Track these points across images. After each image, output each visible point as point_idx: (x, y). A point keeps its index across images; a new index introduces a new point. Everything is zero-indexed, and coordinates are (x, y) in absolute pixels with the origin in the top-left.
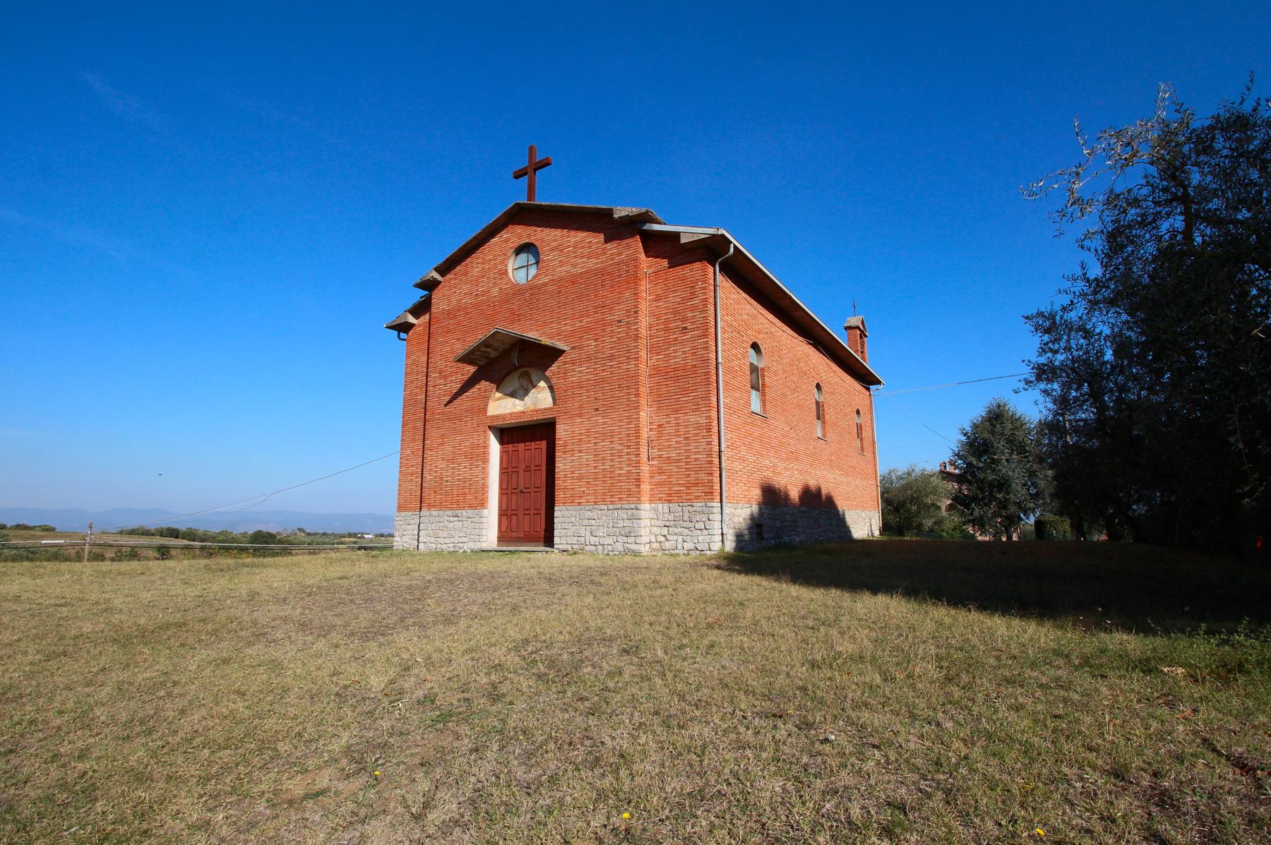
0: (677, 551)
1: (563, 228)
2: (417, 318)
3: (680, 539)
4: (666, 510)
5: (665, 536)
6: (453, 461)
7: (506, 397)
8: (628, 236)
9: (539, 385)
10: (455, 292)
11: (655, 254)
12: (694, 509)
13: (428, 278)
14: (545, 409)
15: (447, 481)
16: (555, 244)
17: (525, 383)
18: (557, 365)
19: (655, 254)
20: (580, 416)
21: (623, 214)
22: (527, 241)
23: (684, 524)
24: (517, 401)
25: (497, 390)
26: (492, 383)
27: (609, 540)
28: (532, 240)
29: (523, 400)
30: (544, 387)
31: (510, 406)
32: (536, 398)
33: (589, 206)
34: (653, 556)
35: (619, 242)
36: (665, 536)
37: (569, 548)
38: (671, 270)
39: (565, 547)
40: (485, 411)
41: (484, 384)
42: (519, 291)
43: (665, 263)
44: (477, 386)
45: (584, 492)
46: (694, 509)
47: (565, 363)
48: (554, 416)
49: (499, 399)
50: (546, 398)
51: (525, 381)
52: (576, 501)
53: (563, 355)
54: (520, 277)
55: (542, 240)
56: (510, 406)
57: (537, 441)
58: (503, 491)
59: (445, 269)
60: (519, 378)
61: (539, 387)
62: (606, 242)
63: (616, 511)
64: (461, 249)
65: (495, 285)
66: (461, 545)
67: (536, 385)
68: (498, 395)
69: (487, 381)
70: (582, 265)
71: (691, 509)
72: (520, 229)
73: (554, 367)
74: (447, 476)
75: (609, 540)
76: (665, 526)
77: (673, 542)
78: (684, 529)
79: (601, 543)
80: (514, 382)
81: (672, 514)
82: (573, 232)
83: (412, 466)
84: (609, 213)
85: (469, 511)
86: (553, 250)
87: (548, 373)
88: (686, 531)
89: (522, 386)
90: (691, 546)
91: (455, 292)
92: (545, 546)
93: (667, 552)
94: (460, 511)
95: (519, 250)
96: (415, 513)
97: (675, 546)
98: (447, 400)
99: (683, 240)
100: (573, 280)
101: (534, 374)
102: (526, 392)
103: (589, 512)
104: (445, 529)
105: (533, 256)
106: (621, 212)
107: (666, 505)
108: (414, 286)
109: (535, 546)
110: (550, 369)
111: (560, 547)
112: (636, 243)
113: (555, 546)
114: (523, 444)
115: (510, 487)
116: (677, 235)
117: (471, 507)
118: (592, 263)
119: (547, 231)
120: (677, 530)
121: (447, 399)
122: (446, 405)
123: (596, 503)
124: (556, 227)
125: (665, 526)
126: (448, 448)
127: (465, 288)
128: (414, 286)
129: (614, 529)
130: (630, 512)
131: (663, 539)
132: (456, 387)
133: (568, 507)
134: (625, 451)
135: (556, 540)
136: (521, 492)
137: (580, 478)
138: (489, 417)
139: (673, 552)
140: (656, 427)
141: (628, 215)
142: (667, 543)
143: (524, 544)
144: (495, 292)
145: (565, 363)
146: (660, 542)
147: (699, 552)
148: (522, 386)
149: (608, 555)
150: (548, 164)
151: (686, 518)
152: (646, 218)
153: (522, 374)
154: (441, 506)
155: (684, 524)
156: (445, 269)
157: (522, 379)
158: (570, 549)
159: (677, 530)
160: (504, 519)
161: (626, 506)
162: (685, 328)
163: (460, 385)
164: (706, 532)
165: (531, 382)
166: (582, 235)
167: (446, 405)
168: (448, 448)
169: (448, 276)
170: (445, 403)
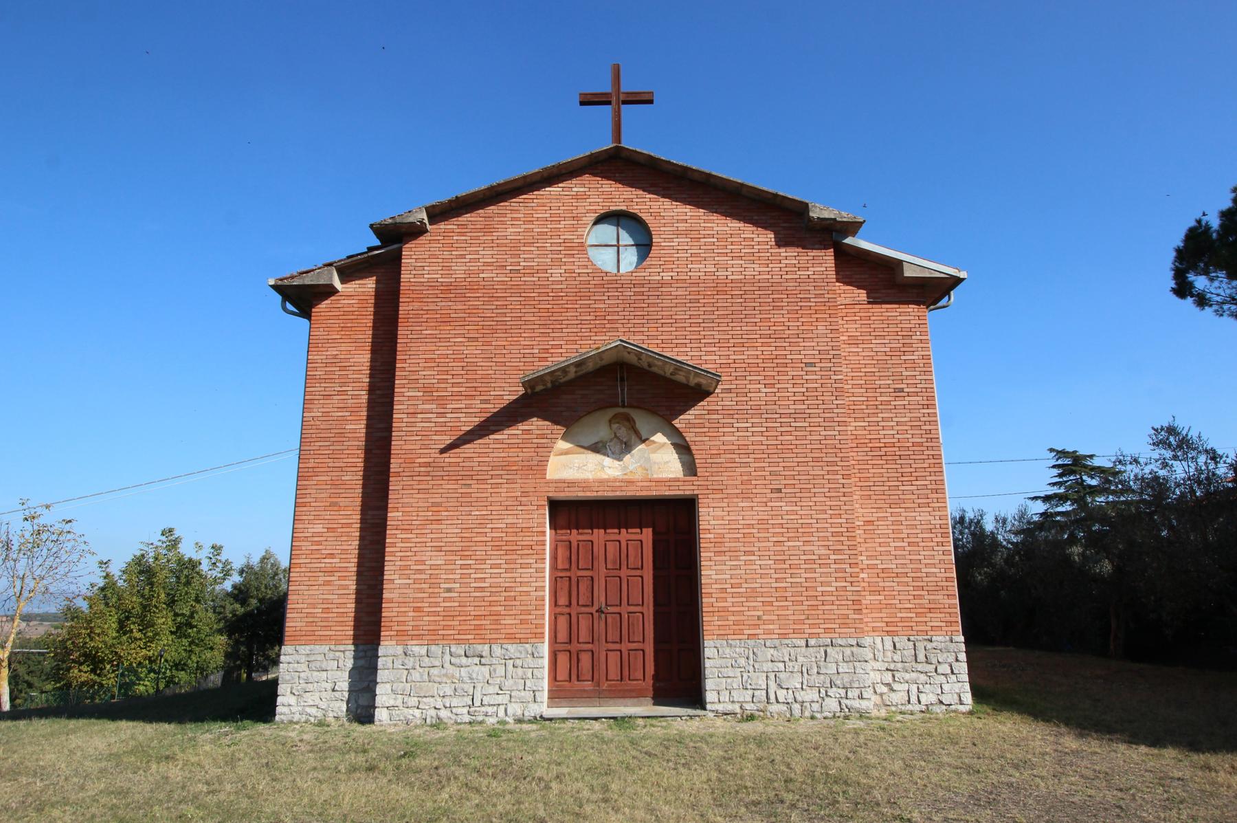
0: (910, 707)
1: (698, 205)
2: (343, 282)
3: (914, 688)
4: (889, 645)
5: (888, 685)
6: (462, 553)
7: (582, 450)
8: (817, 246)
9: (652, 439)
10: (463, 256)
11: (847, 280)
12: (934, 645)
13: (411, 219)
14: (670, 480)
15: (449, 590)
16: (682, 226)
17: (623, 432)
18: (697, 412)
19: (847, 280)
20: (745, 496)
21: (826, 215)
22: (624, 208)
23: (920, 667)
24: (607, 461)
25: (564, 438)
26: (556, 422)
27: (812, 695)
28: (634, 209)
29: (620, 459)
30: (664, 445)
31: (591, 466)
32: (648, 460)
33: (765, 188)
34: (825, 718)
35: (800, 250)
36: (888, 685)
37: (737, 708)
38: (870, 306)
39: (729, 707)
40: (543, 472)
41: (536, 425)
42: (609, 283)
43: (862, 295)
44: (522, 426)
45: (759, 618)
46: (934, 645)
47: (710, 412)
48: (696, 492)
49: (566, 453)
50: (667, 462)
51: (623, 429)
52: (746, 632)
53: (708, 399)
54: (604, 260)
55: (657, 215)
56: (591, 466)
57: (583, 528)
58: (558, 610)
59: (439, 213)
60: (610, 421)
61: (654, 442)
62: (780, 243)
63: (822, 649)
64: (491, 188)
65: (560, 262)
66: (490, 710)
67: (647, 439)
68: (562, 445)
69: (545, 419)
70: (734, 270)
71: (929, 646)
72: (608, 186)
73: (690, 415)
74: (447, 581)
75: (812, 695)
76: (887, 669)
77: (902, 693)
78: (919, 674)
79: (799, 699)
80: (601, 429)
81: (899, 652)
82: (715, 217)
83: (332, 556)
84: (804, 207)
85: (509, 647)
86: (678, 234)
87: (677, 423)
88: (923, 678)
89: (616, 436)
90: (933, 699)
91: (463, 256)
92: (654, 704)
93: (893, 709)
94: (487, 647)
95: (604, 218)
96: (342, 648)
97: (907, 699)
98: (448, 442)
99: (908, 272)
100: (720, 288)
101: (642, 421)
102: (627, 448)
103: (772, 651)
104: (445, 680)
105: (628, 232)
106: (819, 211)
107: (888, 641)
108: (371, 226)
109: (634, 705)
110: (681, 417)
111: (720, 707)
112: (827, 258)
113: (708, 707)
114: (602, 531)
115: (574, 602)
116: (899, 263)
117: (512, 638)
118: (753, 270)
119: (667, 203)
120: (907, 676)
121: (448, 440)
122: (443, 451)
123: (784, 636)
124: (686, 201)
125: (887, 669)
126: (451, 530)
127: (487, 255)
128: (371, 226)
129: (822, 677)
130: (848, 651)
131: (885, 689)
132: (469, 423)
133: (730, 642)
134: (833, 557)
135: (710, 696)
136: (599, 611)
137: (752, 594)
138: (552, 482)
139: (903, 708)
140: (862, 523)
141: (835, 219)
142: (893, 695)
143: (611, 701)
144: (557, 273)
145: (710, 412)
146: (881, 695)
147: (944, 707)
148: (616, 436)
149: (812, 718)
150: (651, 102)
151: (921, 657)
152: (852, 227)
153: (615, 416)
154: (433, 636)
155: (920, 667)
156: (439, 213)
157: (615, 426)
158: (738, 710)
159: (907, 676)
160: (563, 659)
161: (840, 641)
162: (902, 390)
163: (477, 419)
164: (954, 677)
165: (637, 433)
166: (735, 224)
167: (443, 451)
168: (451, 530)
169: (442, 226)
170: (442, 446)
